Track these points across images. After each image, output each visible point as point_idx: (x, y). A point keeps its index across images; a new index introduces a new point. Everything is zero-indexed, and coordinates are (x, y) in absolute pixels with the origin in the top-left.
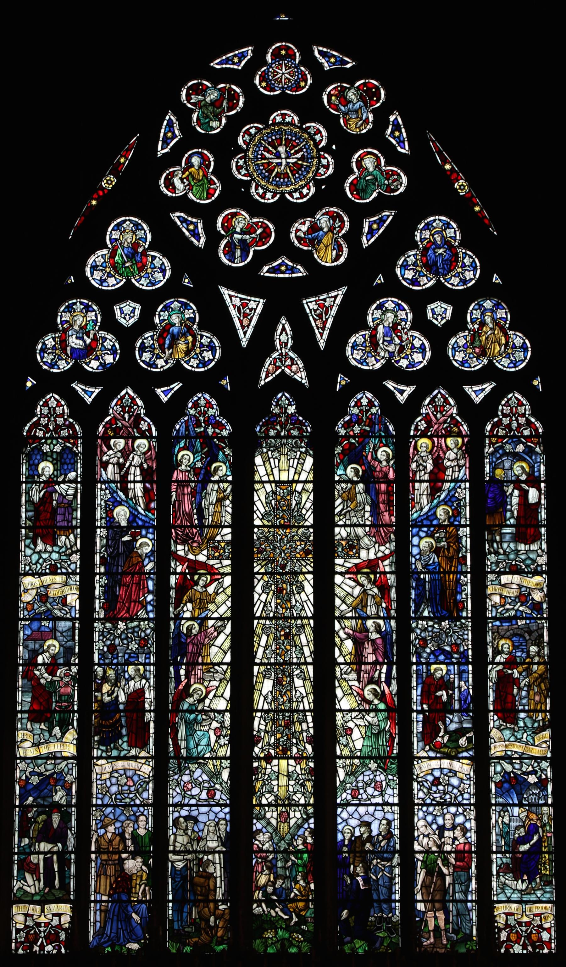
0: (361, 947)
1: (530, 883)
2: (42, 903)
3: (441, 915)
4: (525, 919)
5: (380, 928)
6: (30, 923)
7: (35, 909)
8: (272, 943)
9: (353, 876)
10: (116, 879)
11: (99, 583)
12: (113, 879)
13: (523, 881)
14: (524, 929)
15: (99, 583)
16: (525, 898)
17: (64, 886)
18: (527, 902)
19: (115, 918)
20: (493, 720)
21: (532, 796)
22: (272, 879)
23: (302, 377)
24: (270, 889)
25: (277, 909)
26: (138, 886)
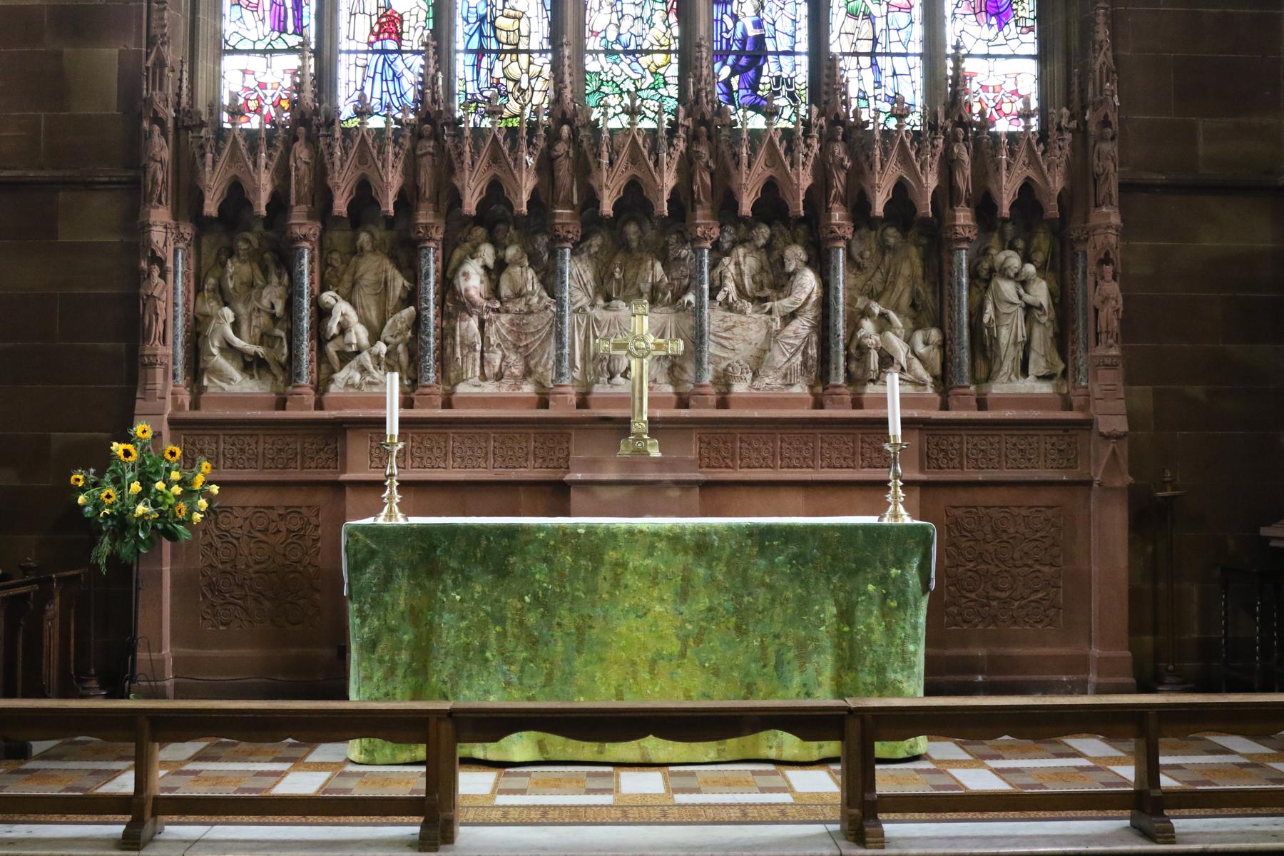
1: (1001, 29)
2: (269, 52)
3: (869, 76)
4: (991, 82)
5: (777, 93)
6: (250, 82)
7: (256, 62)
8: (615, 114)
9: (735, 18)
10: (379, 19)
12: (375, 19)
13: (990, 26)
14: (991, 96)
16: (993, 51)
17: (299, 30)
18: (995, 56)
19: (378, 77)
22: (615, 21)
24: (612, 36)
25: (623, 65)
26: (412, 30)
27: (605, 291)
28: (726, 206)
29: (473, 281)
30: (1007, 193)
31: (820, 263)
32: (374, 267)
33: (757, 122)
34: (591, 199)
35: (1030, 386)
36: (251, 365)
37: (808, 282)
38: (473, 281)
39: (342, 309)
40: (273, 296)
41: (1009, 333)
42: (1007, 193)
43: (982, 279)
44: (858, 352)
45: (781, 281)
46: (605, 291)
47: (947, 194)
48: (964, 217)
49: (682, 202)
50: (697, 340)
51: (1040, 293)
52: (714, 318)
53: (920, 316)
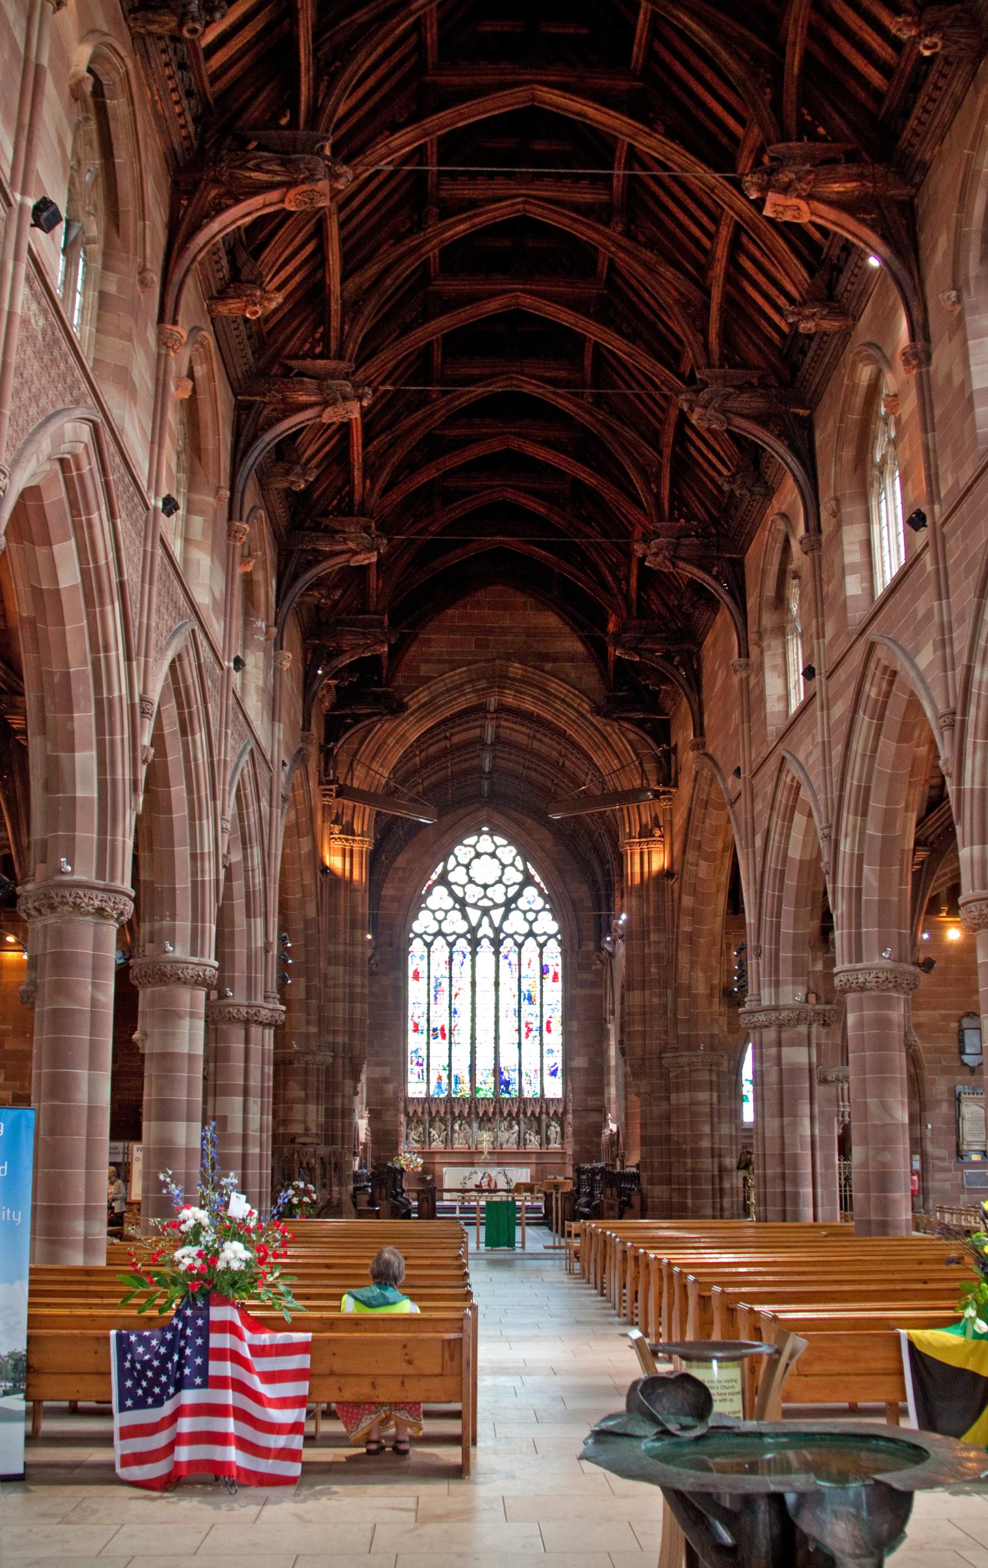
0: (507, 1096)
11: (432, 993)
15: (432, 993)
20: (545, 1032)
21: (555, 1054)
23: (491, 935)
27: (480, 1128)
28: (501, 1113)
29: (456, 1127)
30: (551, 1112)
31: (518, 1124)
32: (438, 1124)
33: (507, 1096)
34: (477, 1113)
35: (557, 1146)
36: (417, 1142)
37: (516, 1127)
38: (456, 1127)
39: (433, 1132)
40: (421, 1129)
41: (553, 1136)
42: (551, 1112)
43: (548, 1126)
44: (525, 1140)
45: (511, 1127)
46: (480, 1128)
47: (541, 1113)
48: (544, 1116)
49: (494, 1113)
50: (496, 1138)
51: (558, 1129)
52: (500, 1134)
53: (538, 1132)
